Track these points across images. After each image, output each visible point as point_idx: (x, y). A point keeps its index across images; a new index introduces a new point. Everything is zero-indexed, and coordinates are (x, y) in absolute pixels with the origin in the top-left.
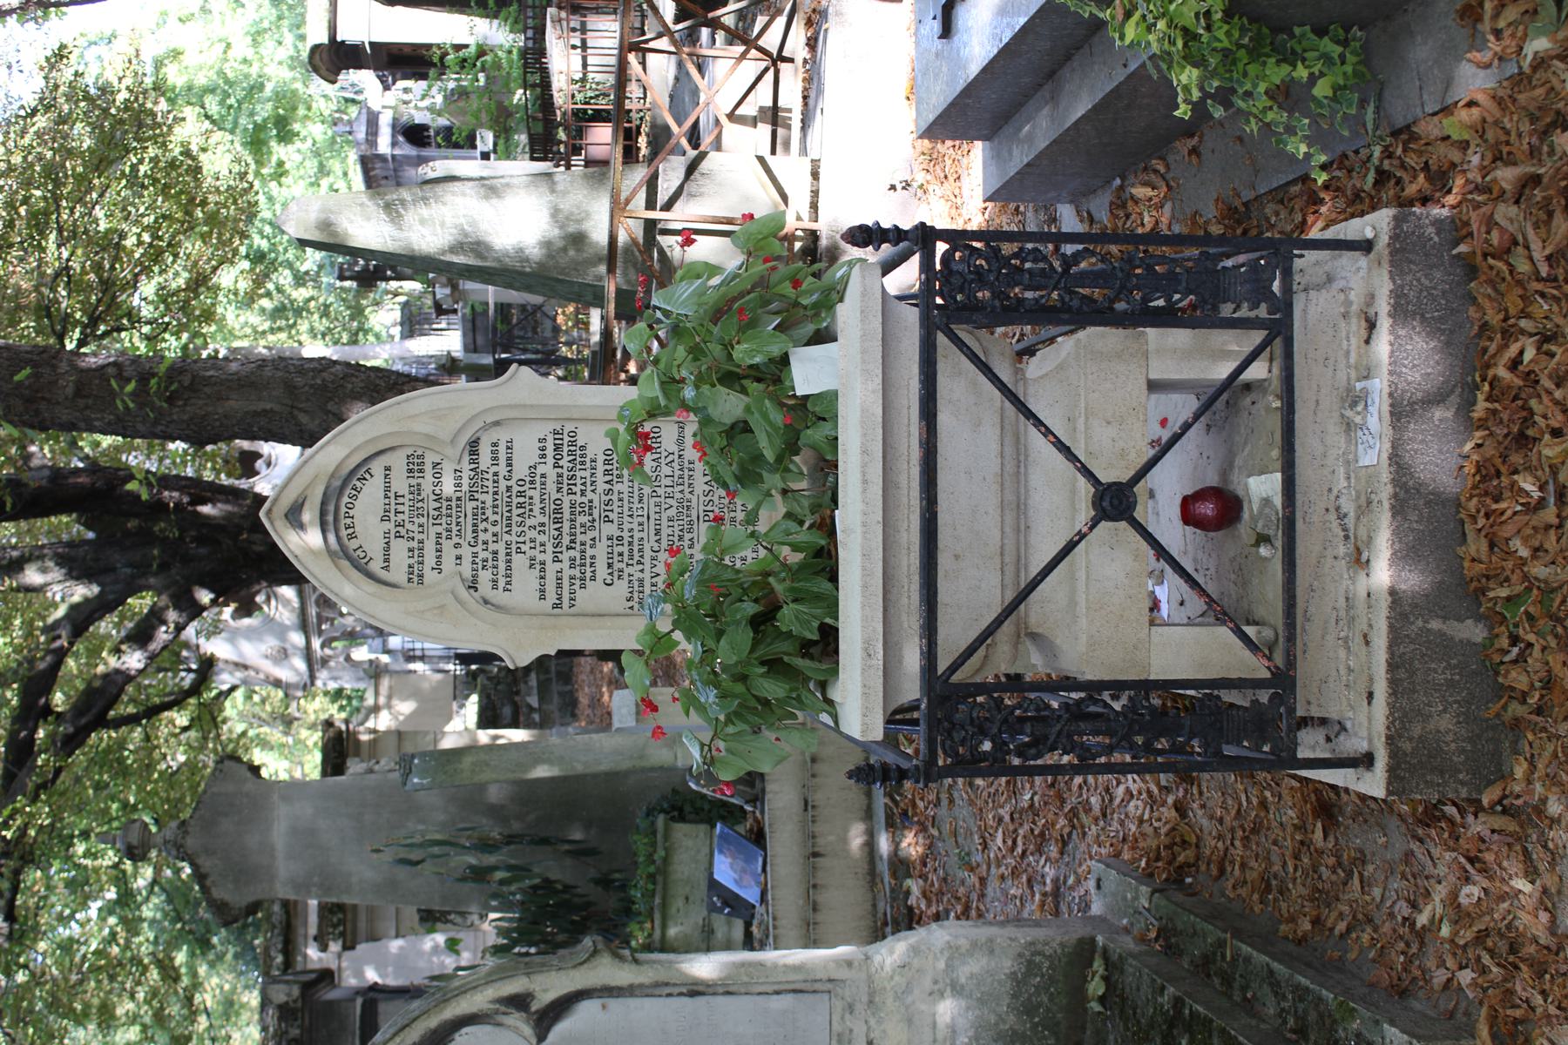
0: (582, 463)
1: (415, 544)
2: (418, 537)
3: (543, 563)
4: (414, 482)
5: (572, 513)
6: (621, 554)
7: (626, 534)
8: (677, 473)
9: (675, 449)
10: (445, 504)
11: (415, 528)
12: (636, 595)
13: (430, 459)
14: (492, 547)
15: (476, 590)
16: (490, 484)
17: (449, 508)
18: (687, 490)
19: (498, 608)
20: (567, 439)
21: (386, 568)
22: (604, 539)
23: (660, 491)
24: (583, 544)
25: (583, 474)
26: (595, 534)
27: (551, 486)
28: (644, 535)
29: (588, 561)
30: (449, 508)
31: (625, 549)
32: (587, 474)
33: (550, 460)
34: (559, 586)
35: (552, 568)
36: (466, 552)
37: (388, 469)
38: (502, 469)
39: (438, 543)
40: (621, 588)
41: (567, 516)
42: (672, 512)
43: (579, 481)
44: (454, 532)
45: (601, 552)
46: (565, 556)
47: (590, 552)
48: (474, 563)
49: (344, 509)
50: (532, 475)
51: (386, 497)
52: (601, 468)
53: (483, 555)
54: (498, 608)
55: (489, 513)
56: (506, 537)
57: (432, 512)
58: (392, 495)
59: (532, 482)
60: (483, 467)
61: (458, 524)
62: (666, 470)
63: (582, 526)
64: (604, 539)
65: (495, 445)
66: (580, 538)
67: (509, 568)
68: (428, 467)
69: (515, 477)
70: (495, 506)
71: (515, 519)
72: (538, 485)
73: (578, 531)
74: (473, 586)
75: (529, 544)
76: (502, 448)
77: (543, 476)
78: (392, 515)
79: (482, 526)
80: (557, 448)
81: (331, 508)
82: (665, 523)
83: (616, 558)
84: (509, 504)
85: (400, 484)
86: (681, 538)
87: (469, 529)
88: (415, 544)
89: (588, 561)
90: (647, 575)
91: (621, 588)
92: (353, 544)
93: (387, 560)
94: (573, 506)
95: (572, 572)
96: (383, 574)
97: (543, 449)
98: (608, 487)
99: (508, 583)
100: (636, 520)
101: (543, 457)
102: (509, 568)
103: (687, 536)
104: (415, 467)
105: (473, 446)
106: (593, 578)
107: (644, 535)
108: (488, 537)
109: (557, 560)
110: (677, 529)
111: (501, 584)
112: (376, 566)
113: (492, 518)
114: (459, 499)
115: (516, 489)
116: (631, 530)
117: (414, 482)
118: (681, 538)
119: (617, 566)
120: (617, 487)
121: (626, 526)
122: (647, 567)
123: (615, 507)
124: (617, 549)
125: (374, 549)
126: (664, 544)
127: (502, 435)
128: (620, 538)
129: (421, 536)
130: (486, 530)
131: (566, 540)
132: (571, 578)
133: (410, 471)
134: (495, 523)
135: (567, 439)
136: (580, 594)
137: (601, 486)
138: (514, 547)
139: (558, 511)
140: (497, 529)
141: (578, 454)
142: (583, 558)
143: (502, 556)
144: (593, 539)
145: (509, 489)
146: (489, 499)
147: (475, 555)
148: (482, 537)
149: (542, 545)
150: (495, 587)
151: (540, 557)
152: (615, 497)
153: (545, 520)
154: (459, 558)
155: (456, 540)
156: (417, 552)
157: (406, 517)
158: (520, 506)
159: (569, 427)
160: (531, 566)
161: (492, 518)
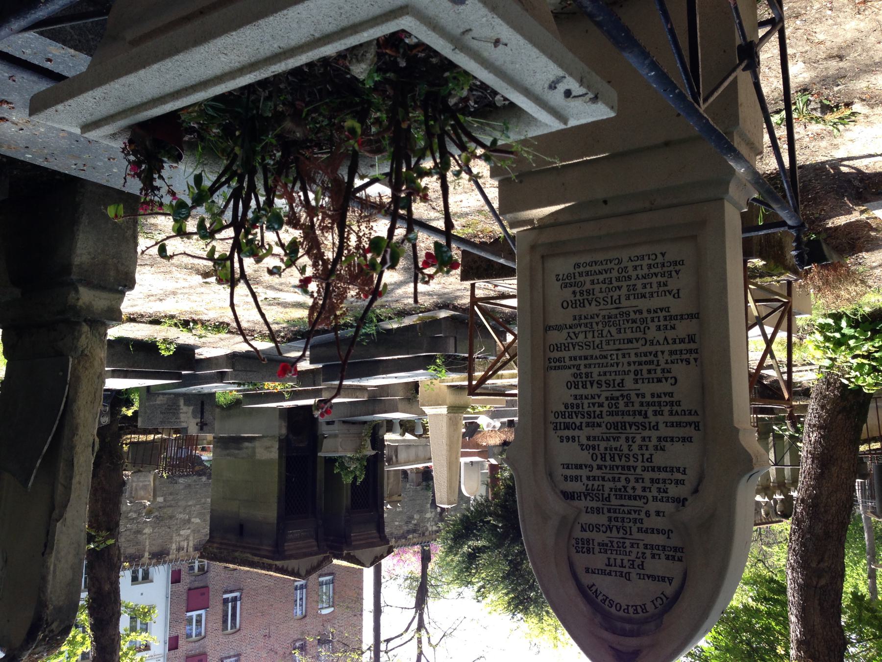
0: (578, 407)
1: (648, 553)
2: (642, 549)
3: (659, 439)
4: (597, 549)
5: (617, 414)
6: (649, 372)
7: (633, 368)
8: (583, 329)
9: (565, 333)
10: (613, 523)
11: (635, 551)
12: (684, 357)
13: (578, 534)
14: (647, 484)
15: (685, 499)
16: (596, 483)
17: (616, 519)
18: (596, 320)
19: (700, 481)
20: (560, 420)
21: (670, 580)
22: (637, 386)
23: (597, 341)
24: (642, 404)
25: (586, 406)
26: (633, 393)
27: (597, 432)
28: (633, 352)
29: (656, 399)
30: (616, 519)
31: (645, 368)
32: (586, 402)
33: (576, 433)
34: (679, 424)
35: (664, 431)
36: (652, 506)
37: (587, 570)
38: (584, 473)
39: (646, 532)
40: (678, 370)
41: (619, 419)
42: (613, 330)
43: (592, 409)
44: (636, 516)
45: (648, 389)
46: (652, 419)
47: (648, 398)
48: (662, 500)
49: (621, 613)
50: (588, 447)
51: (610, 574)
52: (581, 391)
53: (655, 493)
54: (700, 481)
55: (619, 485)
56: (639, 471)
57: (621, 535)
58: (608, 569)
59: (594, 449)
60: (583, 489)
61: (629, 513)
62: (581, 337)
63: (627, 405)
64: (637, 386)
65: (566, 478)
66: (637, 407)
67: (665, 469)
68: (586, 535)
69: (590, 462)
70: (614, 478)
71: (623, 463)
72: (596, 443)
73: (631, 409)
74: (681, 502)
75: (644, 452)
76: (569, 472)
77: (588, 438)
78: (625, 570)
79: (630, 492)
80: (567, 427)
81: (619, 624)
82: (622, 336)
83: (653, 375)
84: (611, 468)
85: (599, 560)
86: (634, 321)
87: (632, 503)
88: (648, 553)
89: (656, 399)
90: (667, 348)
91: (678, 370)
92: (650, 608)
93: (663, 579)
94: (611, 414)
95: (666, 413)
96: (676, 584)
97: (568, 439)
98: (595, 385)
99: (678, 470)
100: (621, 360)
101: (573, 438)
102: (665, 469)
103: (633, 316)
104: (585, 546)
105: (568, 496)
106: (671, 394)
107: (633, 352)
108: (639, 486)
109: (656, 427)
110: (627, 325)
111: (679, 476)
112: (670, 590)
113: (623, 483)
114: (609, 511)
115: (599, 462)
116: (629, 364)
117: (597, 549)
118: (634, 321)
119: (659, 374)
120: (595, 377)
121: (626, 368)
122: (659, 348)
123: (611, 378)
124: (646, 375)
125: (655, 589)
126: (639, 335)
127: (560, 472)
128: (636, 373)
129: (641, 546)
130: (634, 488)
131: (639, 419)
132: (671, 414)
133: (588, 551)
134: (628, 480)
135: (560, 420)
136: (685, 406)
137: (595, 390)
138: (647, 464)
139: (615, 426)
140: (632, 478)
141: (572, 409)
142: (653, 404)
143: (655, 475)
144: (638, 395)
145: (599, 467)
146: (608, 485)
147: (655, 499)
148: (639, 492)
149: (644, 439)
150: (682, 482)
151: (654, 441)
152: (603, 378)
153: (623, 436)
154: (658, 513)
155: (643, 515)
156: (655, 551)
157: (626, 558)
158: (612, 458)
159: (552, 418)
160: (663, 449)
161: (623, 483)
